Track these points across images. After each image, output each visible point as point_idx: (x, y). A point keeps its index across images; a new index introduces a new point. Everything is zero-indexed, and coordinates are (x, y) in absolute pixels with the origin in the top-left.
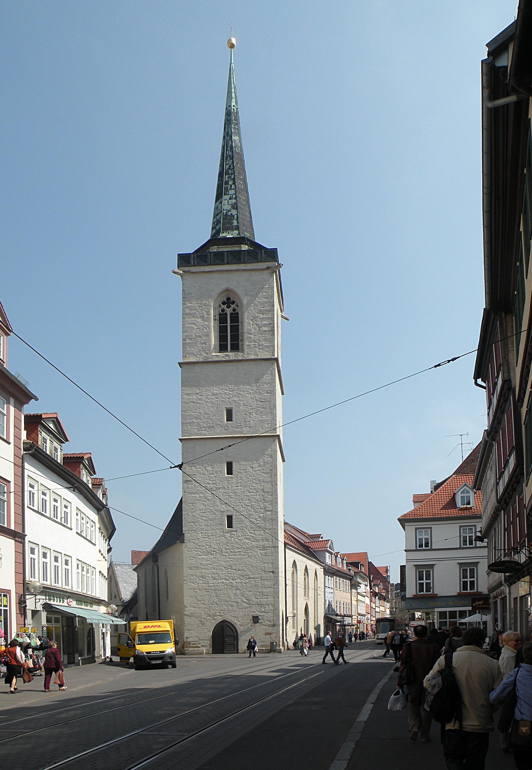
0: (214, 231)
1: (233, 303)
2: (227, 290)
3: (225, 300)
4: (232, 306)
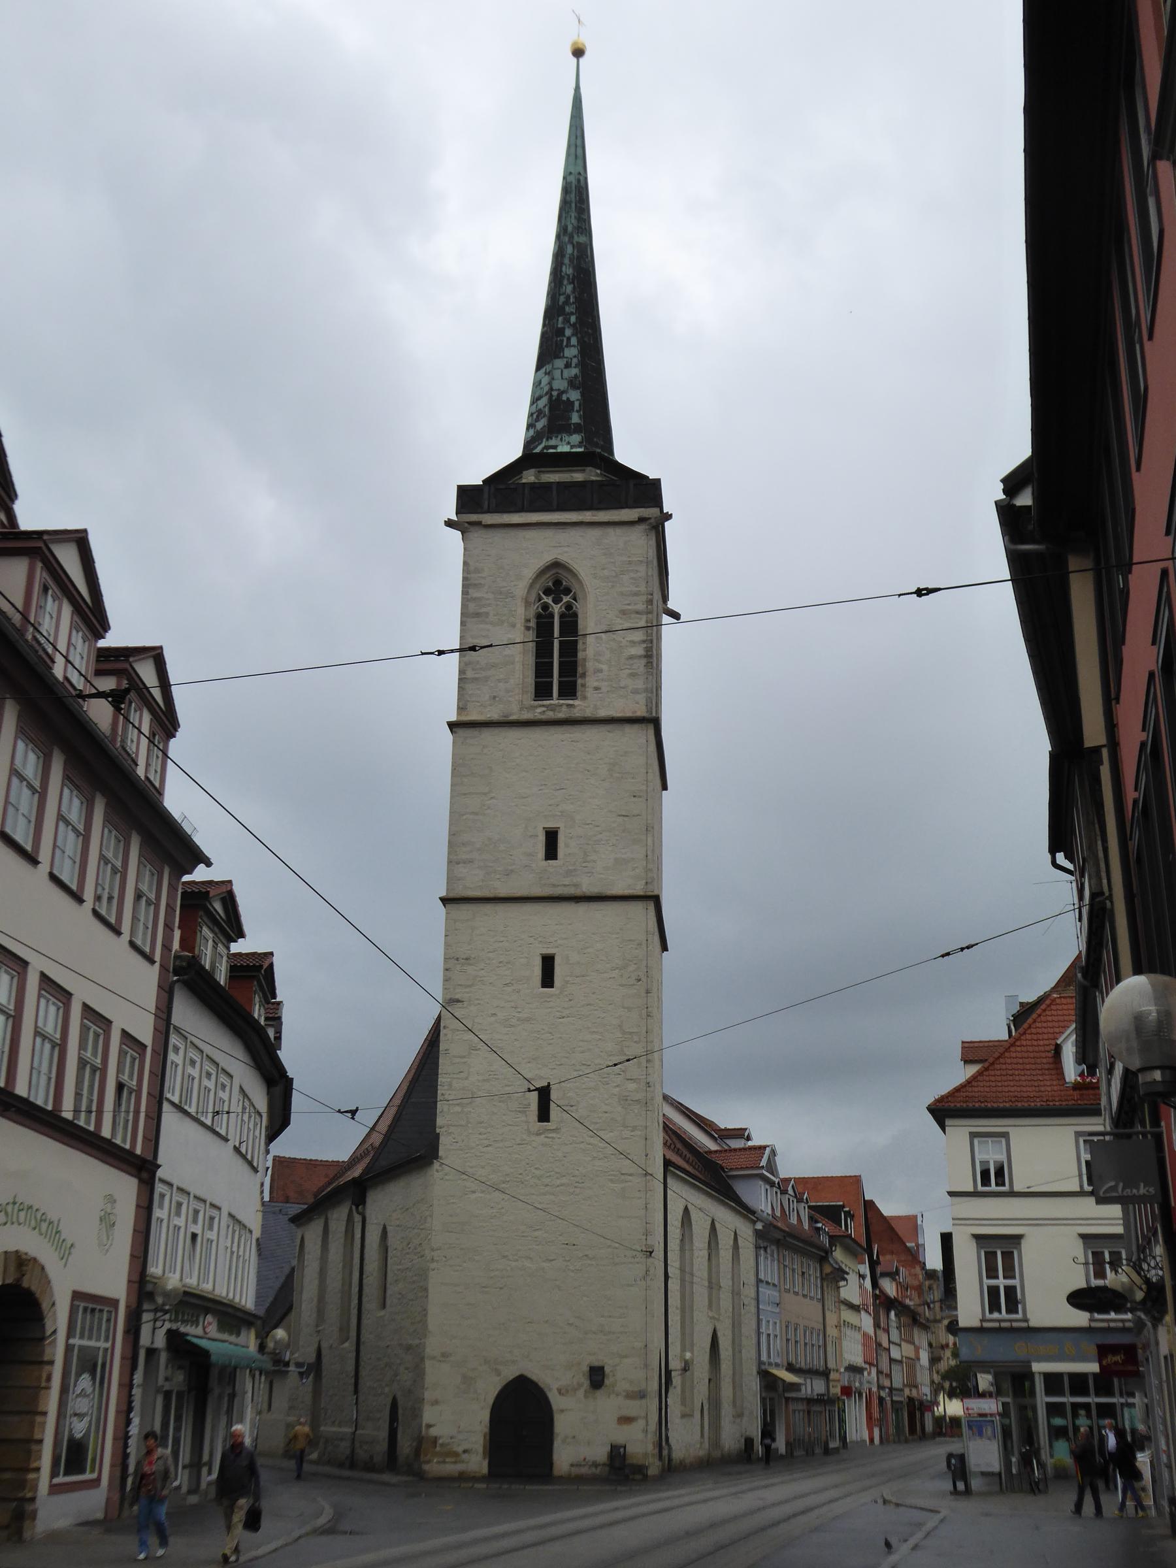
0: (532, 432)
1: (567, 591)
2: (556, 565)
3: (550, 584)
4: (566, 599)
